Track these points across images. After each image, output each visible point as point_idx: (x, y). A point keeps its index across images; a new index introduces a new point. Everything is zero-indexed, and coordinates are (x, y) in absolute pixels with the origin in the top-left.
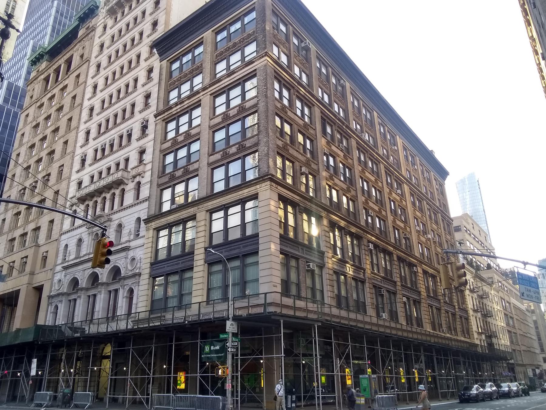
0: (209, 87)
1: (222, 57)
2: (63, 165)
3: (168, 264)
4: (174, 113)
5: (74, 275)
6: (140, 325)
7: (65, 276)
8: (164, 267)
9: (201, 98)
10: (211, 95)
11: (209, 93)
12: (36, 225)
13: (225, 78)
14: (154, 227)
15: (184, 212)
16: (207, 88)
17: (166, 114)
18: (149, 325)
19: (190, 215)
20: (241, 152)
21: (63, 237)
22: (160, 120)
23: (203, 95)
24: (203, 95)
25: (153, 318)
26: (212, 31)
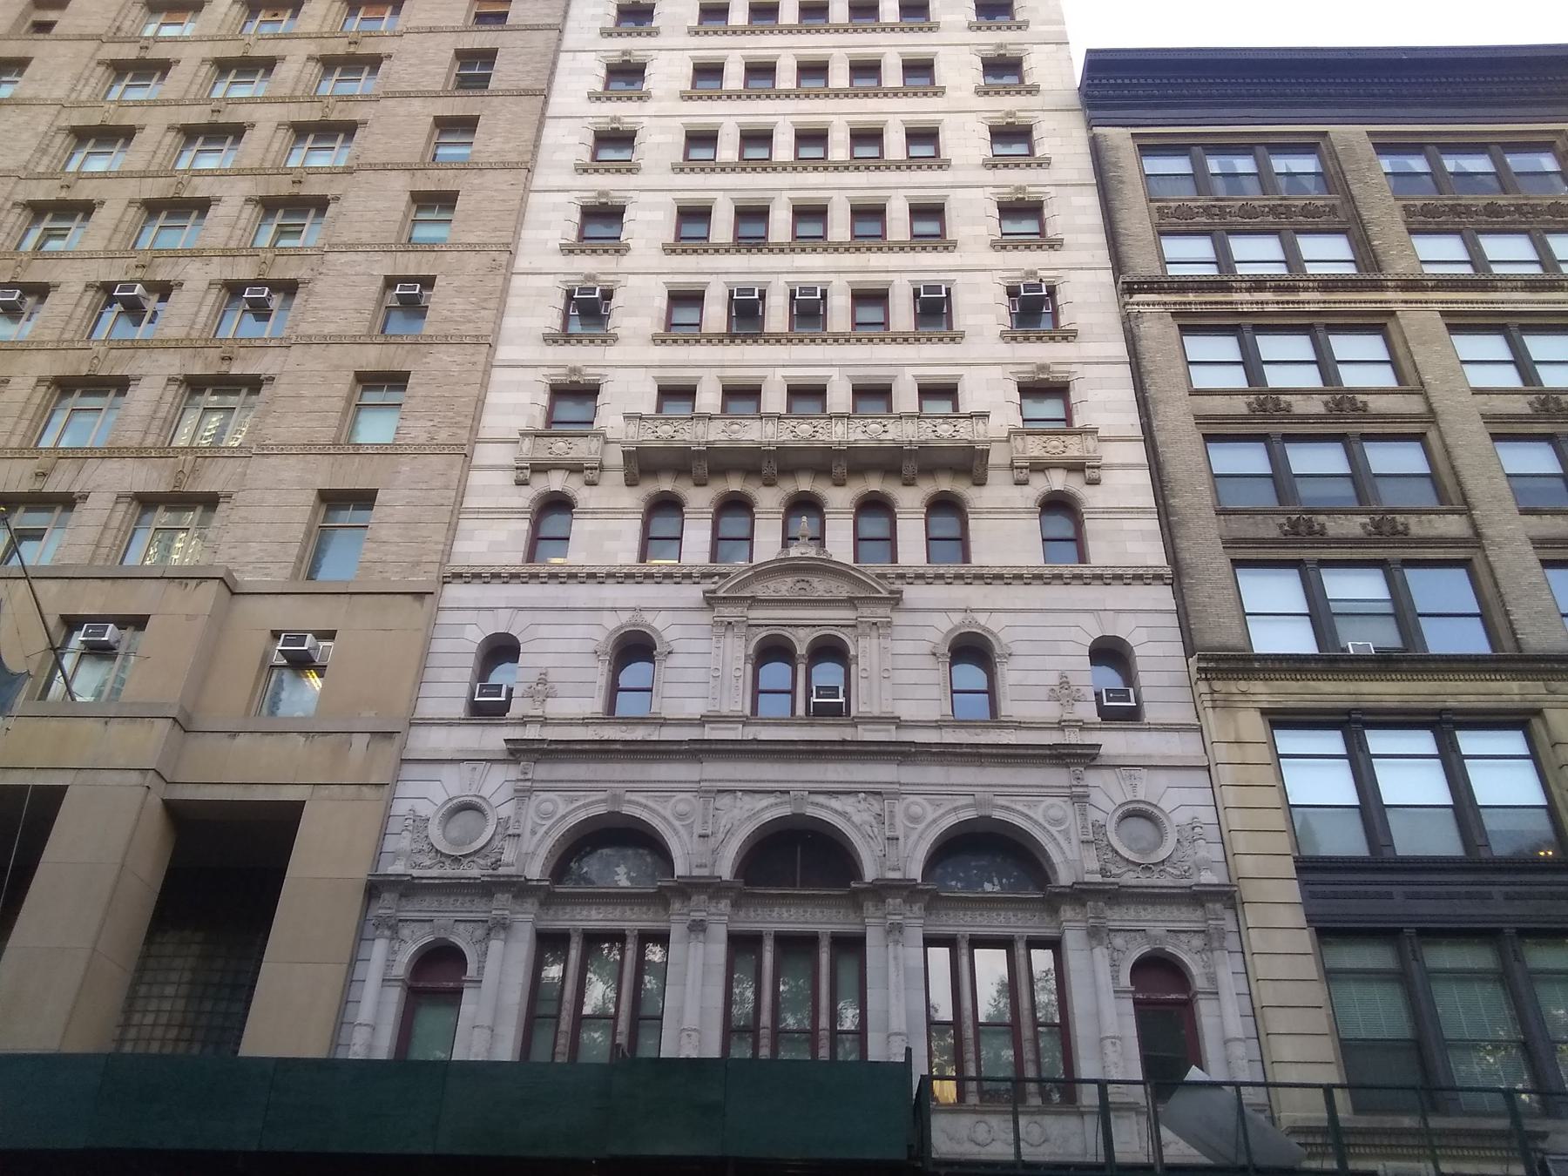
0: (1435, 289)
1: (1430, 223)
2: (428, 282)
3: (1514, 884)
4: (1246, 308)
5: (616, 798)
6: (1360, 1156)
7: (523, 794)
8: (1389, 896)
9: (1394, 307)
10: (1444, 314)
11: (1444, 307)
12: (179, 482)
13: (1514, 289)
14: (1266, 701)
15: (1462, 686)
16: (1424, 289)
17: (1191, 297)
18: (1342, 1162)
19: (1503, 705)
20: (1376, 544)
21: (455, 593)
22: (1158, 309)
23: (1406, 302)
24: (1406, 302)
25: (1443, 1133)
26: (1370, 134)
